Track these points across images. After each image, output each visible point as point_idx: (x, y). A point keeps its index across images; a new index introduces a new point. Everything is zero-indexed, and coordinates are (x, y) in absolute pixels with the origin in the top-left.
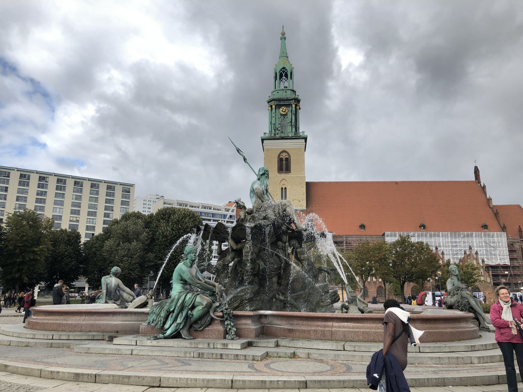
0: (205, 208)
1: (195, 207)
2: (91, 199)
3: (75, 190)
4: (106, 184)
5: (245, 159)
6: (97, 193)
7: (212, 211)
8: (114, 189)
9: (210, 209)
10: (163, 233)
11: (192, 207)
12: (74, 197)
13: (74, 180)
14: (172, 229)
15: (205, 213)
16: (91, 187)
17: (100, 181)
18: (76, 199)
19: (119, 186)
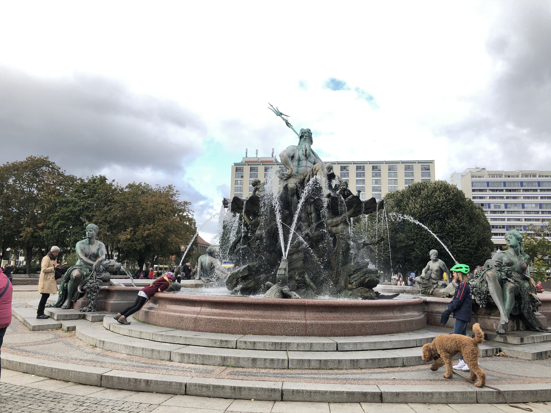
0: (526, 176)
1: (513, 176)
2: (390, 181)
3: (374, 174)
4: (404, 165)
5: (287, 124)
6: (396, 175)
7: (537, 179)
8: (413, 168)
9: (534, 176)
10: (411, 211)
11: (509, 176)
12: (374, 181)
13: (371, 165)
14: (421, 206)
15: (528, 182)
16: (389, 170)
17: (397, 162)
18: (376, 183)
19: (384, 165)
